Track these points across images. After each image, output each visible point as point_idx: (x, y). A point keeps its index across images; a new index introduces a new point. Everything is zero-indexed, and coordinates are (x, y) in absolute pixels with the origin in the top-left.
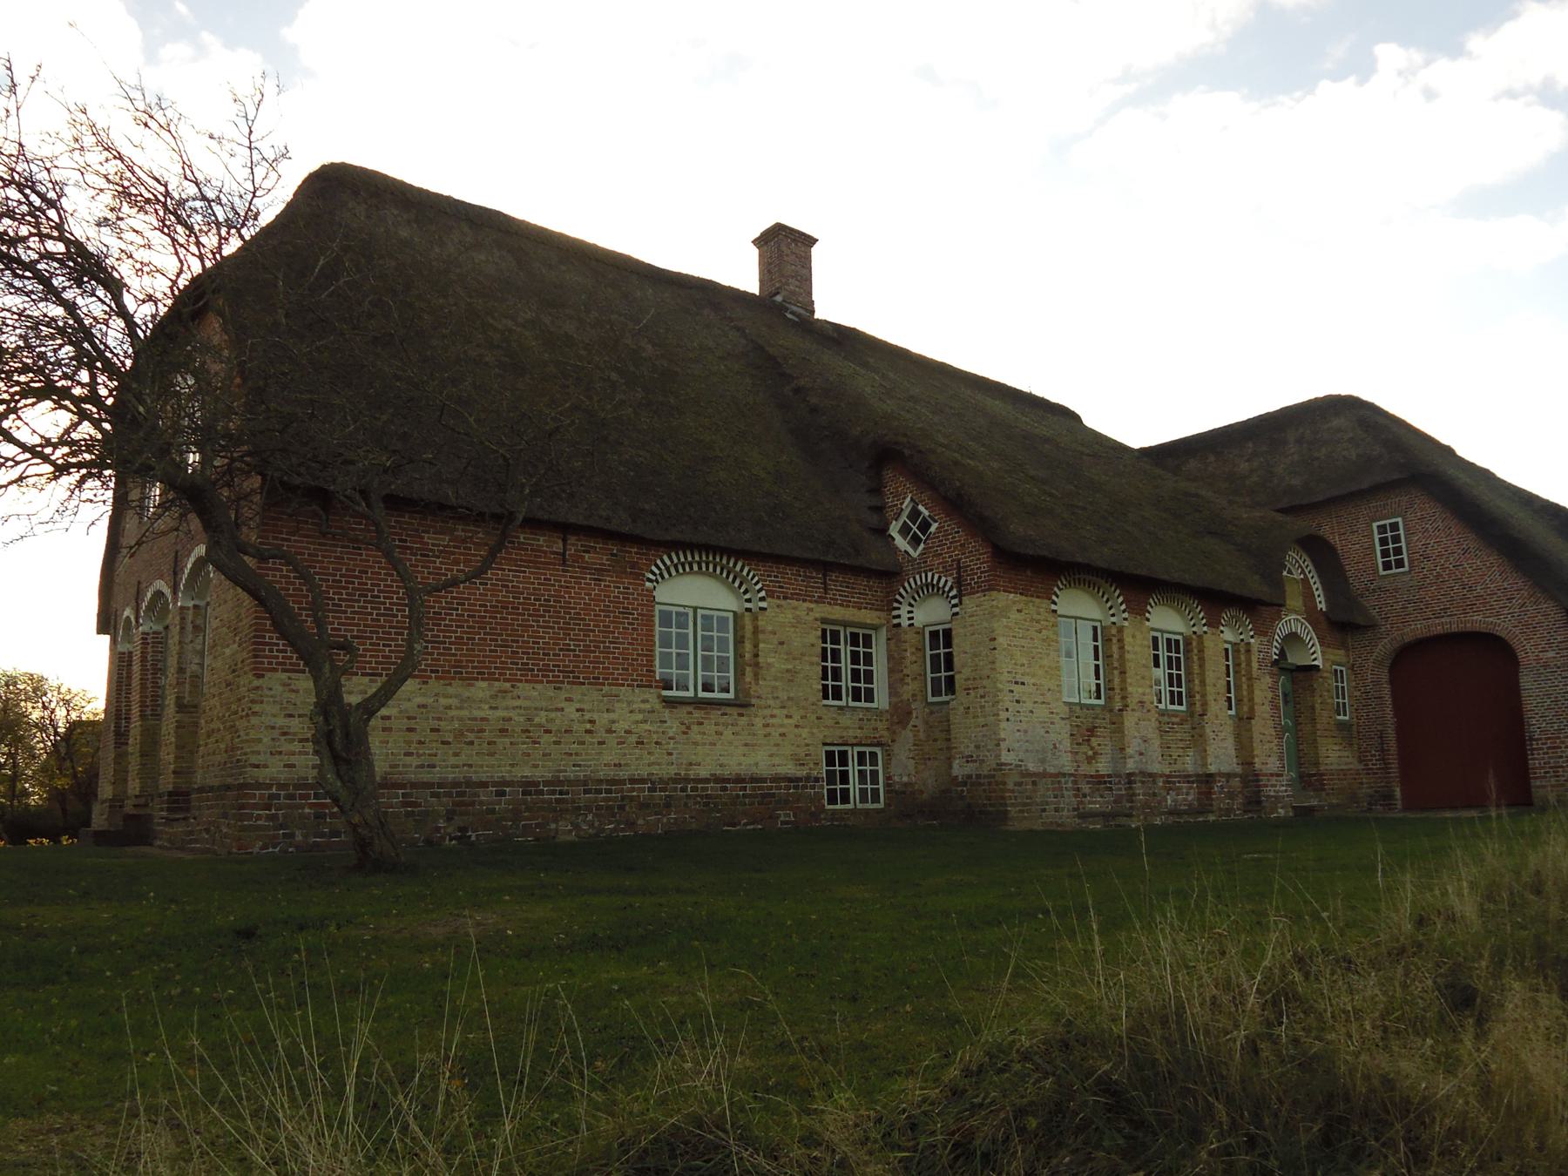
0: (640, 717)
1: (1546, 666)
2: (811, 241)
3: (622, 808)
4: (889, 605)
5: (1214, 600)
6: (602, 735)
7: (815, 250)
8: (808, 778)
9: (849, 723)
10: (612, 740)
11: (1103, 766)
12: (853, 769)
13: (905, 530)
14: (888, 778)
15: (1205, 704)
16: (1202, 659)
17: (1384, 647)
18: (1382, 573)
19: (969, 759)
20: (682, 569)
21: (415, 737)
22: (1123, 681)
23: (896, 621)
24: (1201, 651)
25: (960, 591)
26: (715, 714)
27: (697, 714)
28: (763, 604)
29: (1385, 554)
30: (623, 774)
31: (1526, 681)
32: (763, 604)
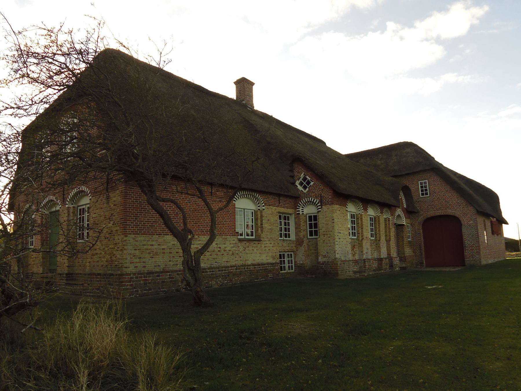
0: (233, 245)
1: (470, 226)
3: (228, 275)
4: (295, 207)
5: (383, 205)
7: (254, 87)
9: (285, 245)
10: (225, 254)
12: (286, 259)
13: (301, 184)
14: (295, 262)
15: (380, 237)
16: (379, 223)
17: (421, 219)
18: (421, 196)
19: (325, 256)
20: (243, 196)
21: (172, 255)
22: (362, 231)
23: (298, 212)
24: (379, 221)
25: (321, 204)
26: (252, 243)
28: (264, 208)
29: (422, 191)
30: (229, 265)
31: (464, 230)
32: (264, 208)
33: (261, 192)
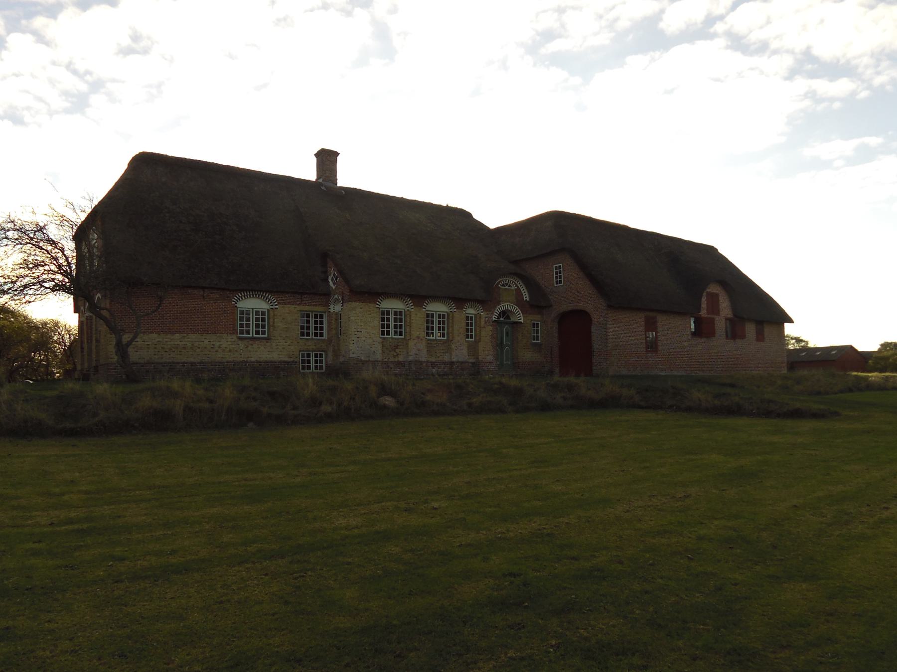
2: (336, 154)
4: (327, 305)
11: (401, 359)
12: (313, 359)
14: (326, 362)
20: (246, 297)
27: (251, 342)
31: (593, 329)
33: (271, 292)
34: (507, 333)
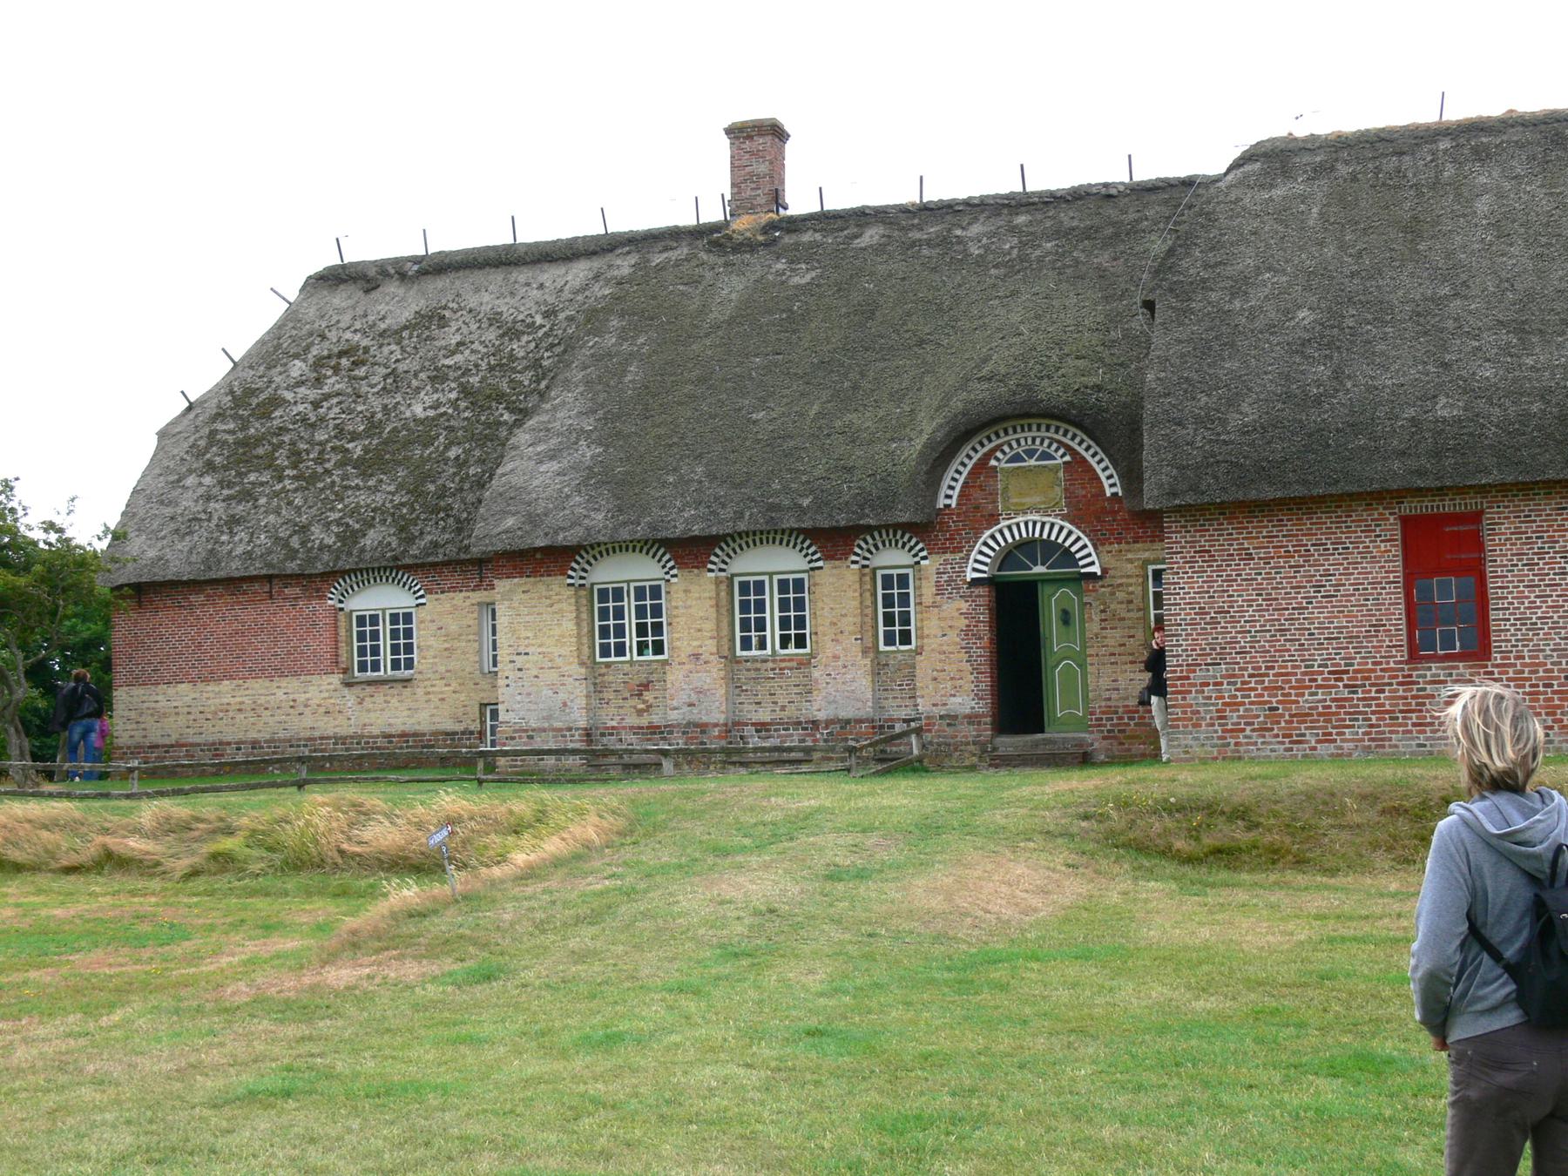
6: (301, 709)
8: (463, 733)
10: (307, 711)
11: (656, 718)
27: (369, 690)
30: (317, 734)
34: (1066, 618)
